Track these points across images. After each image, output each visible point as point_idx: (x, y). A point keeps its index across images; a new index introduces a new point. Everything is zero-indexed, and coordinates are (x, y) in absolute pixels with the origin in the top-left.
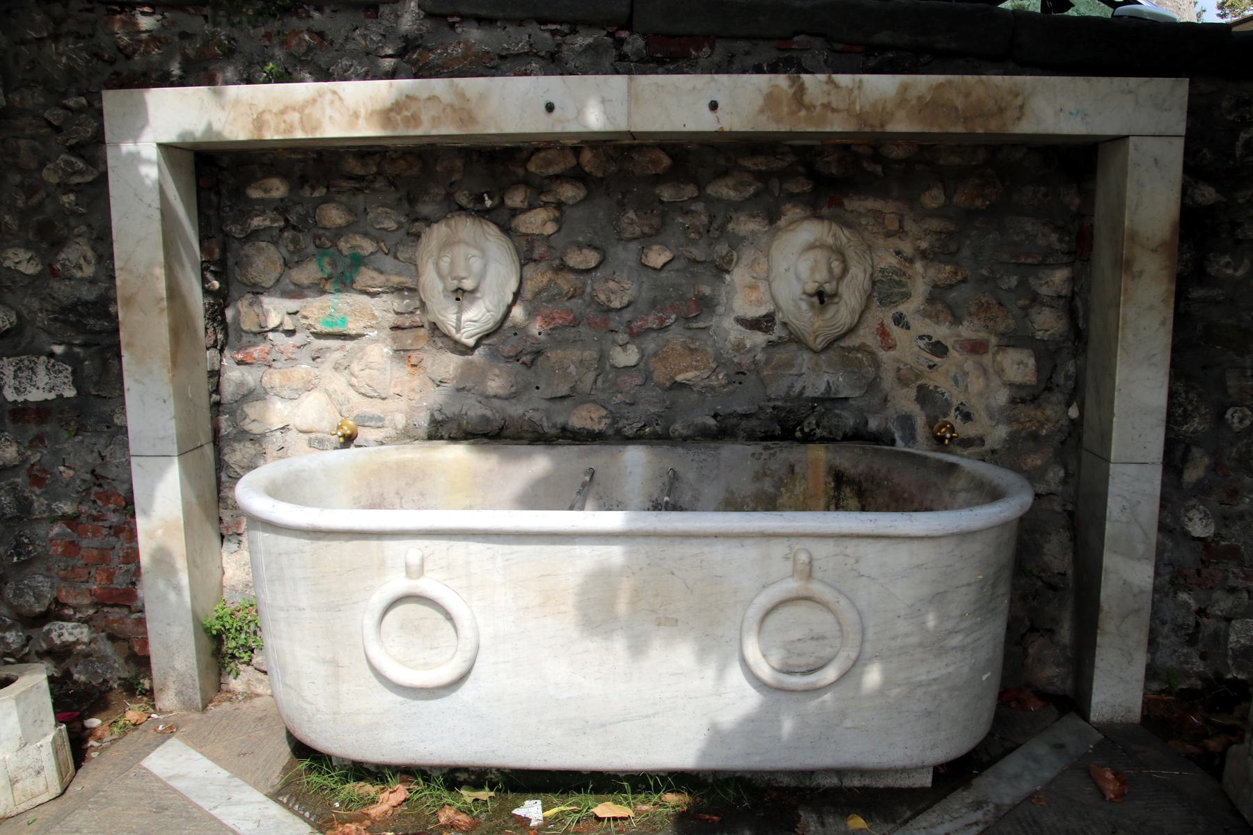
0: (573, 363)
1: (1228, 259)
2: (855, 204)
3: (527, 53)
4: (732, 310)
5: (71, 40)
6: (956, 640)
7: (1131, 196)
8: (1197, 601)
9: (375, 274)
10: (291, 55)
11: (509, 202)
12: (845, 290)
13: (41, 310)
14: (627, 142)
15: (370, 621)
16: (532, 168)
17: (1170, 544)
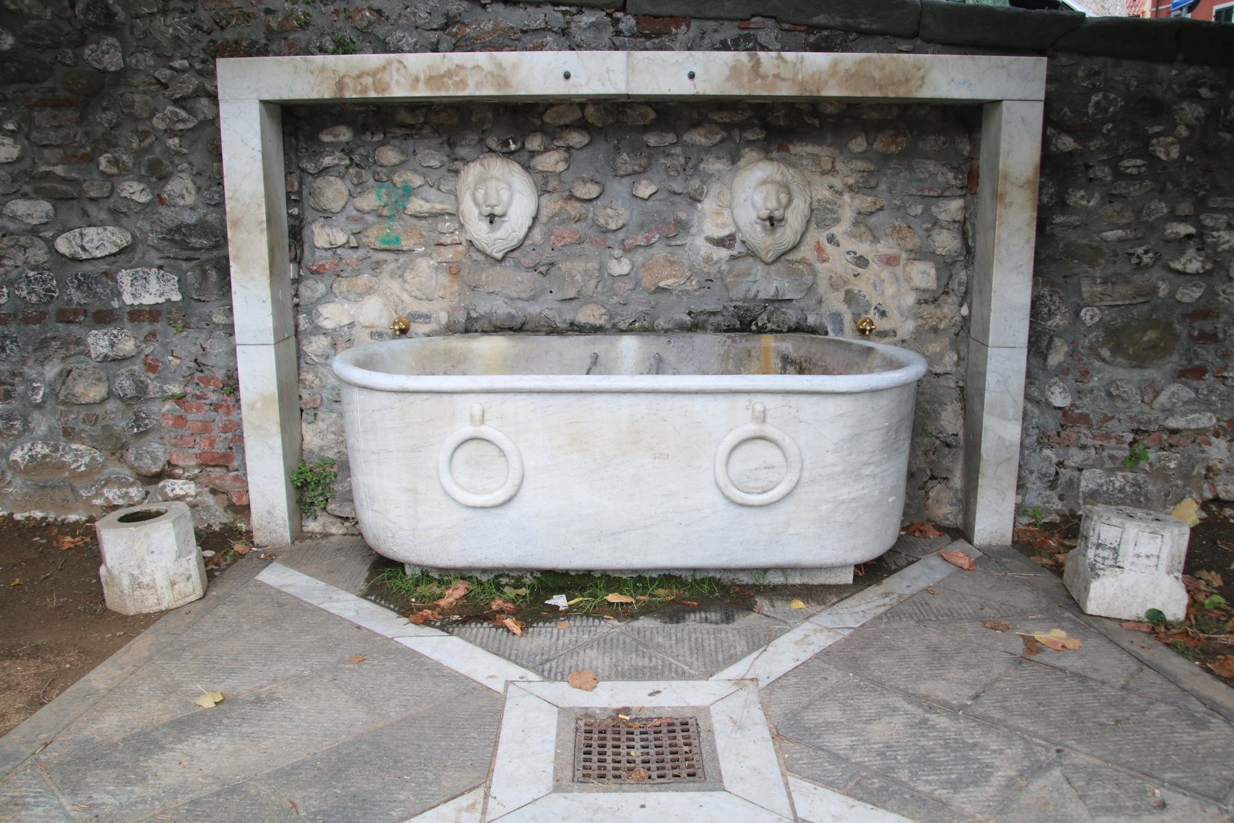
1: (1082, 193)
2: (797, 149)
3: (543, 29)
4: (702, 231)
5: (177, 15)
6: (869, 470)
7: (1004, 145)
8: (1057, 456)
10: (355, 28)
11: (529, 146)
13: (152, 231)
15: (443, 458)
16: (547, 119)
17: (1037, 412)
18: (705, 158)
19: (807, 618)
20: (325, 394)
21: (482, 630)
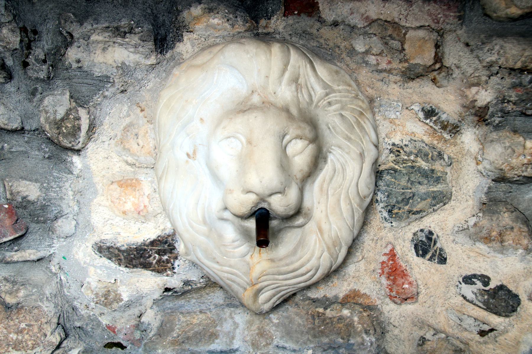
4: (89, 227)
12: (315, 198)
18: (77, 31)
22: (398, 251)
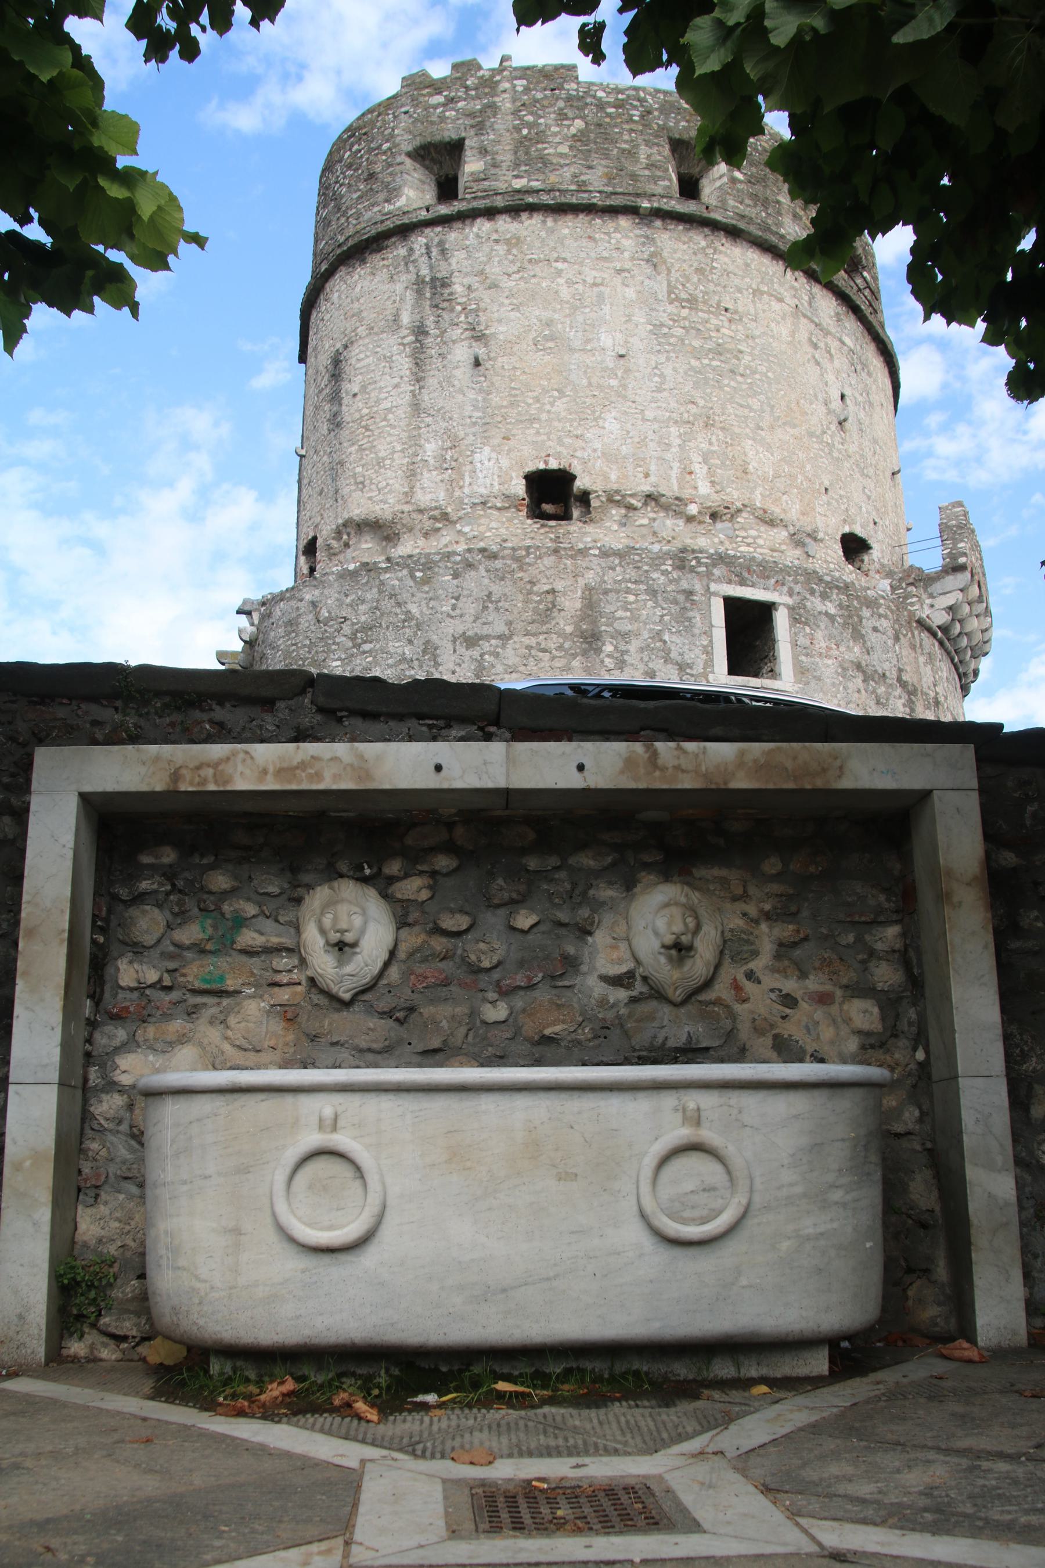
0: (445, 1018)
1: (1036, 913)
2: (701, 872)
4: (595, 968)
6: (837, 1195)
7: (941, 838)
9: (256, 935)
12: (698, 943)
14: (498, 813)
15: (280, 1177)
17: (1029, 1178)
18: (594, 883)
19: (777, 1402)
20: (112, 1169)
21: (321, 1420)
22: (738, 978)
